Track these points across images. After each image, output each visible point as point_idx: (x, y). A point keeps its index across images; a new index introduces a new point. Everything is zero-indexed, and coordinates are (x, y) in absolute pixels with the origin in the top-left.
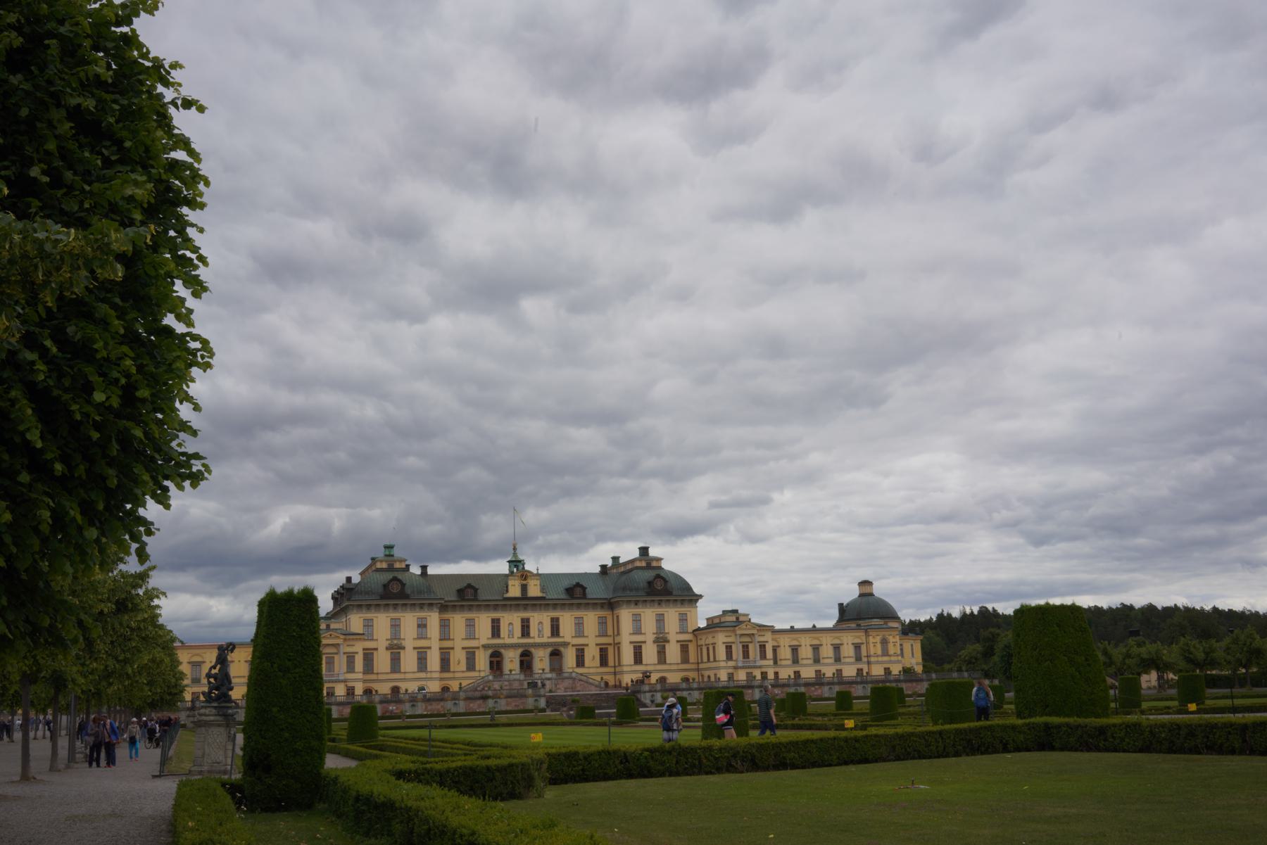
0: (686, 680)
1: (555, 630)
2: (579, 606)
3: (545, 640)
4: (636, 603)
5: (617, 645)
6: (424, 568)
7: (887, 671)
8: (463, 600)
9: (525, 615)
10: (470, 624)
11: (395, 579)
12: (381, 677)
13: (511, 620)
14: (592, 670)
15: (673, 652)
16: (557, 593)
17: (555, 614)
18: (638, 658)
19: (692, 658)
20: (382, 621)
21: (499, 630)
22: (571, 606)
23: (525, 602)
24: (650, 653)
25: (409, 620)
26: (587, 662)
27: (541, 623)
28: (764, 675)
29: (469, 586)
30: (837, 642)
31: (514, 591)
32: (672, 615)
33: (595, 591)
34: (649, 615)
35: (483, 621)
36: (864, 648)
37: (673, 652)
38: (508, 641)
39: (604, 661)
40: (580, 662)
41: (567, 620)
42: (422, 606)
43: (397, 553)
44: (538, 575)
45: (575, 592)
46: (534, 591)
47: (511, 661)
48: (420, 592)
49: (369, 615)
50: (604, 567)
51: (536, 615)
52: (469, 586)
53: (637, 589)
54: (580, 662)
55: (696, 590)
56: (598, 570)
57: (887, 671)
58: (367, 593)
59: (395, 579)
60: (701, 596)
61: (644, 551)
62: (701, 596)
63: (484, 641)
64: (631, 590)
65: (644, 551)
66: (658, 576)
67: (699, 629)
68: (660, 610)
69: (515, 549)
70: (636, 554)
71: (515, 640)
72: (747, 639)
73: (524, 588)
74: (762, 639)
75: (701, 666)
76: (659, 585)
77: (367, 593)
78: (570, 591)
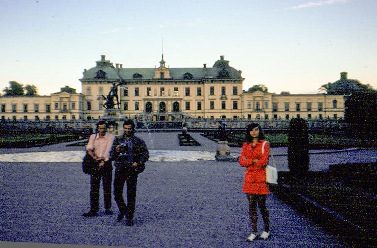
0: (235, 117)
2: (188, 83)
6: (121, 65)
7: (335, 116)
9: (162, 86)
12: (95, 112)
13: (155, 88)
15: (229, 104)
16: (180, 76)
18: (212, 107)
20: (95, 88)
23: (162, 80)
24: (218, 105)
27: (169, 90)
30: (309, 101)
31: (158, 76)
32: (229, 87)
34: (218, 87)
35: (143, 89)
36: (324, 104)
37: (229, 104)
38: (154, 97)
39: (199, 107)
40: (188, 107)
43: (106, 59)
44: (169, 68)
45: (188, 77)
47: (156, 108)
49: (89, 86)
50: (205, 65)
51: (166, 86)
54: (188, 107)
56: (203, 66)
57: (335, 116)
60: (244, 79)
61: (222, 57)
62: (244, 79)
65: (222, 57)
70: (220, 59)
71: (156, 97)
73: (162, 74)
74: (266, 99)
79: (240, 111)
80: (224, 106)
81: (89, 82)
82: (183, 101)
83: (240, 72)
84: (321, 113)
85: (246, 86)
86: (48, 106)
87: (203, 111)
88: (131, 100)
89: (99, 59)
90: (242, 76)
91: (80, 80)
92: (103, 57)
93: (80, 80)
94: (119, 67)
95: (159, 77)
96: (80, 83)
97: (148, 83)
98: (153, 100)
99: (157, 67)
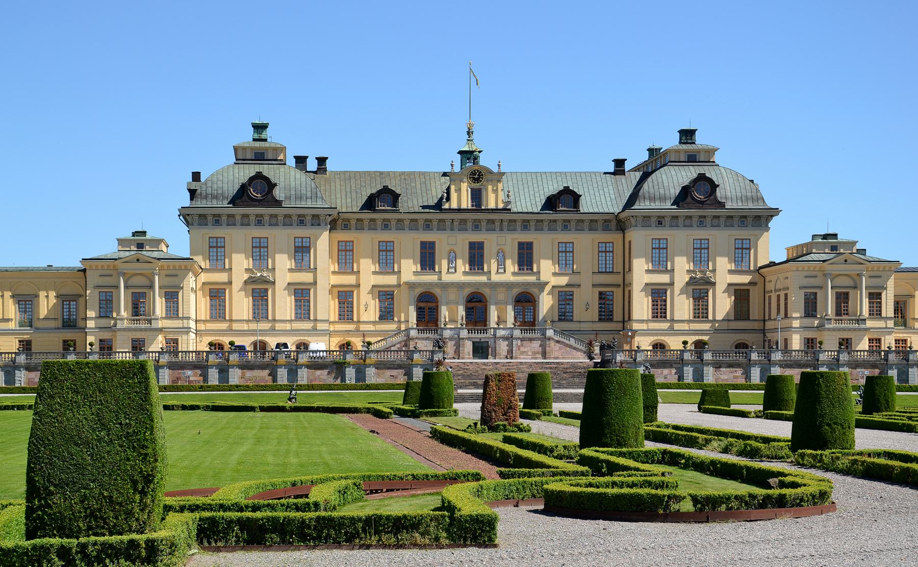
5: (626, 286)
6: (322, 161)
8: (375, 211)
15: (722, 305)
18: (660, 310)
22: (552, 226)
29: (386, 190)
39: (606, 314)
43: (273, 136)
46: (491, 201)
49: (218, 232)
53: (663, 199)
55: (771, 204)
56: (611, 168)
58: (215, 197)
60: (775, 212)
61: (687, 135)
62: (775, 212)
64: (652, 199)
65: (687, 135)
67: (772, 264)
69: (469, 133)
72: (847, 282)
73: (477, 196)
75: (769, 325)
77: (215, 197)
78: (551, 203)
80: (701, 312)
81: (217, 220)
82: (548, 288)
87: (756, 325)
88: (365, 287)
89: (246, 137)
92: (260, 128)
94: (312, 165)
95: (467, 203)
97: (428, 226)
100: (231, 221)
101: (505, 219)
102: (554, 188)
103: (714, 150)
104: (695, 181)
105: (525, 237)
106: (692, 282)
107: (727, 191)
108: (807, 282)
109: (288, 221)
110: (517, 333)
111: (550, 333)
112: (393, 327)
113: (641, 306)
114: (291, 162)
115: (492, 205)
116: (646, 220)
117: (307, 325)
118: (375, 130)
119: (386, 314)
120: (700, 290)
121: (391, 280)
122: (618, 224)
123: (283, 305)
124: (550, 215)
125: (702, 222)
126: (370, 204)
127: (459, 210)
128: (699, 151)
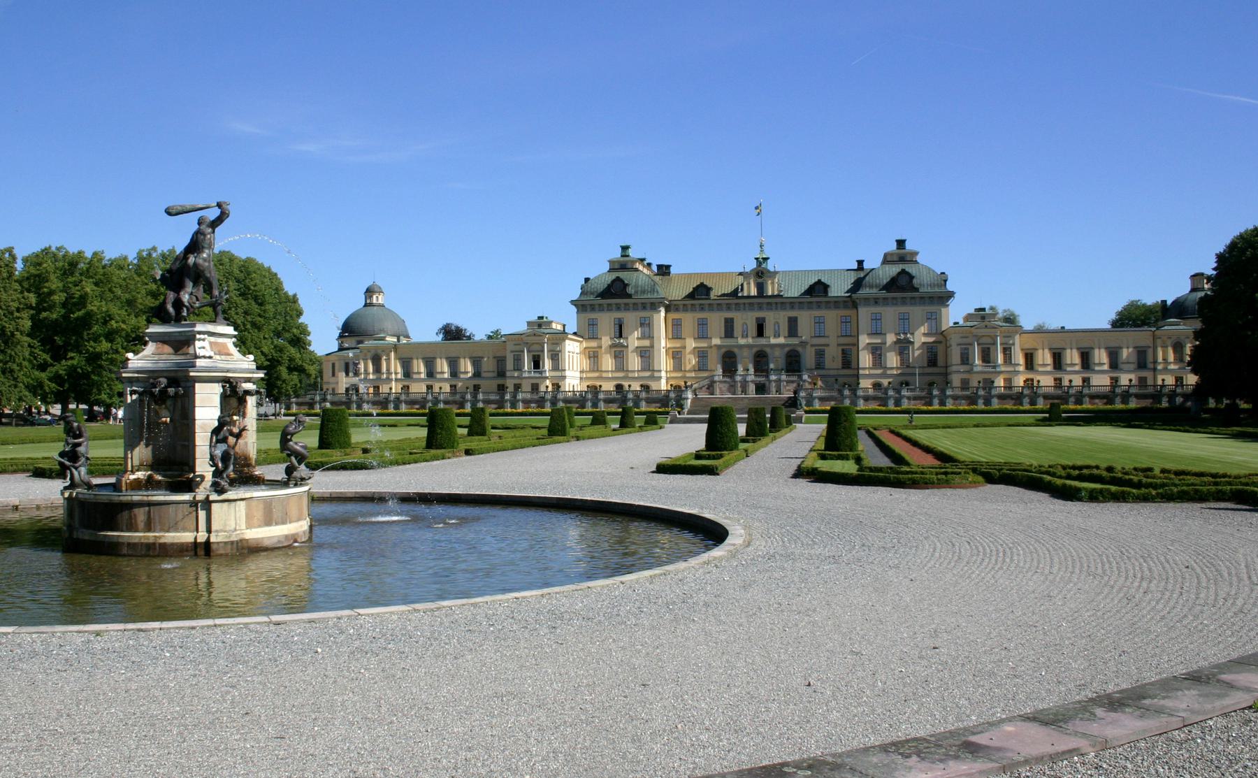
1: (793, 329)
2: (818, 306)
3: (781, 340)
4: (876, 302)
5: (857, 345)
6: (668, 267)
10: (702, 324)
11: (618, 279)
12: (604, 375)
13: (745, 320)
14: (832, 373)
17: (793, 314)
19: (941, 362)
20: (606, 320)
21: (732, 327)
22: (810, 306)
25: (630, 318)
26: (828, 363)
28: (1008, 381)
29: (702, 285)
33: (839, 289)
34: (890, 314)
36: (1150, 352)
41: (806, 319)
42: (644, 307)
45: (818, 289)
48: (643, 292)
49: (593, 315)
50: (860, 263)
52: (702, 285)
59: (618, 279)
61: (901, 243)
62: (951, 295)
63: (716, 341)
64: (871, 287)
65: (901, 243)
66: (903, 271)
68: (903, 309)
69: (761, 246)
71: (750, 341)
72: (989, 340)
73: (761, 287)
75: (950, 369)
76: (903, 281)
79: (943, 370)
81: (593, 308)
82: (808, 347)
83: (944, 279)
84: (1144, 374)
85: (955, 313)
86: (501, 361)
88: (689, 349)
89: (617, 254)
90: (950, 287)
91: (572, 302)
92: (625, 248)
93: (572, 302)
95: (754, 292)
96: (574, 309)
97: (729, 308)
98: (741, 347)
99: (748, 270)
100: (601, 308)
101: (779, 302)
102: (813, 280)
103: (916, 253)
104: (899, 274)
105: (793, 314)
106: (898, 341)
107: (921, 278)
108: (961, 341)
109: (635, 307)
110: (784, 377)
111: (805, 377)
112: (705, 374)
113: (865, 359)
114: (655, 268)
115: (770, 293)
116: (867, 301)
117: (647, 374)
118: (704, 247)
119: (701, 367)
120: (903, 346)
121: (704, 344)
122: (851, 301)
123: (634, 362)
124: (808, 299)
125: (904, 302)
126: (691, 296)
127: (749, 297)
128: (906, 254)
